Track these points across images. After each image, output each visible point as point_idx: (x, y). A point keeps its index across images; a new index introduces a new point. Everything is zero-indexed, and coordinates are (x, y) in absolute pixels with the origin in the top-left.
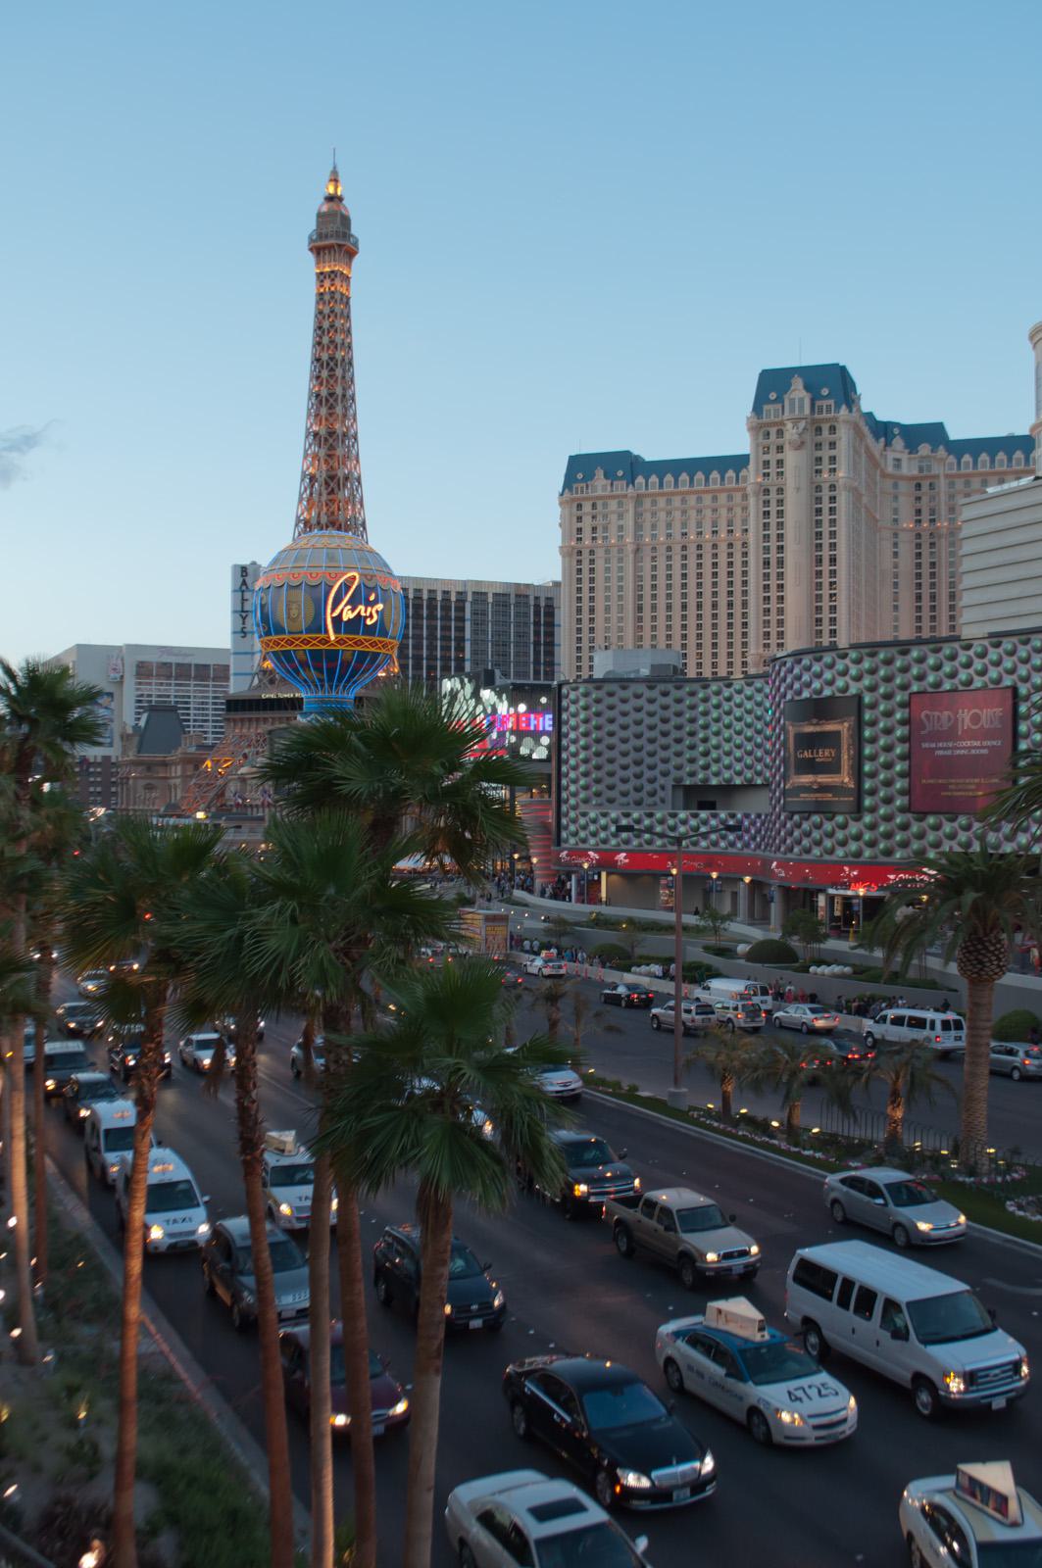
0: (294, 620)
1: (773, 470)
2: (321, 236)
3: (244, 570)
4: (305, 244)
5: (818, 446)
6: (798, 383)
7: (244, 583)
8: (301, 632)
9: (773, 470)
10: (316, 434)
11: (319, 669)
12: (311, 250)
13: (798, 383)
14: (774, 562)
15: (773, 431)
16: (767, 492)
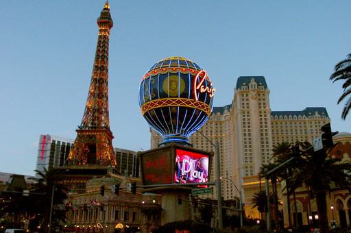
0: (173, 90)
1: (246, 106)
2: (101, 18)
3: (45, 137)
4: (96, 21)
5: (260, 99)
6: (253, 80)
7: (44, 141)
8: (177, 97)
9: (246, 106)
10: (95, 79)
11: (181, 119)
12: (98, 23)
13: (253, 80)
14: (247, 135)
15: (245, 94)
16: (244, 112)
